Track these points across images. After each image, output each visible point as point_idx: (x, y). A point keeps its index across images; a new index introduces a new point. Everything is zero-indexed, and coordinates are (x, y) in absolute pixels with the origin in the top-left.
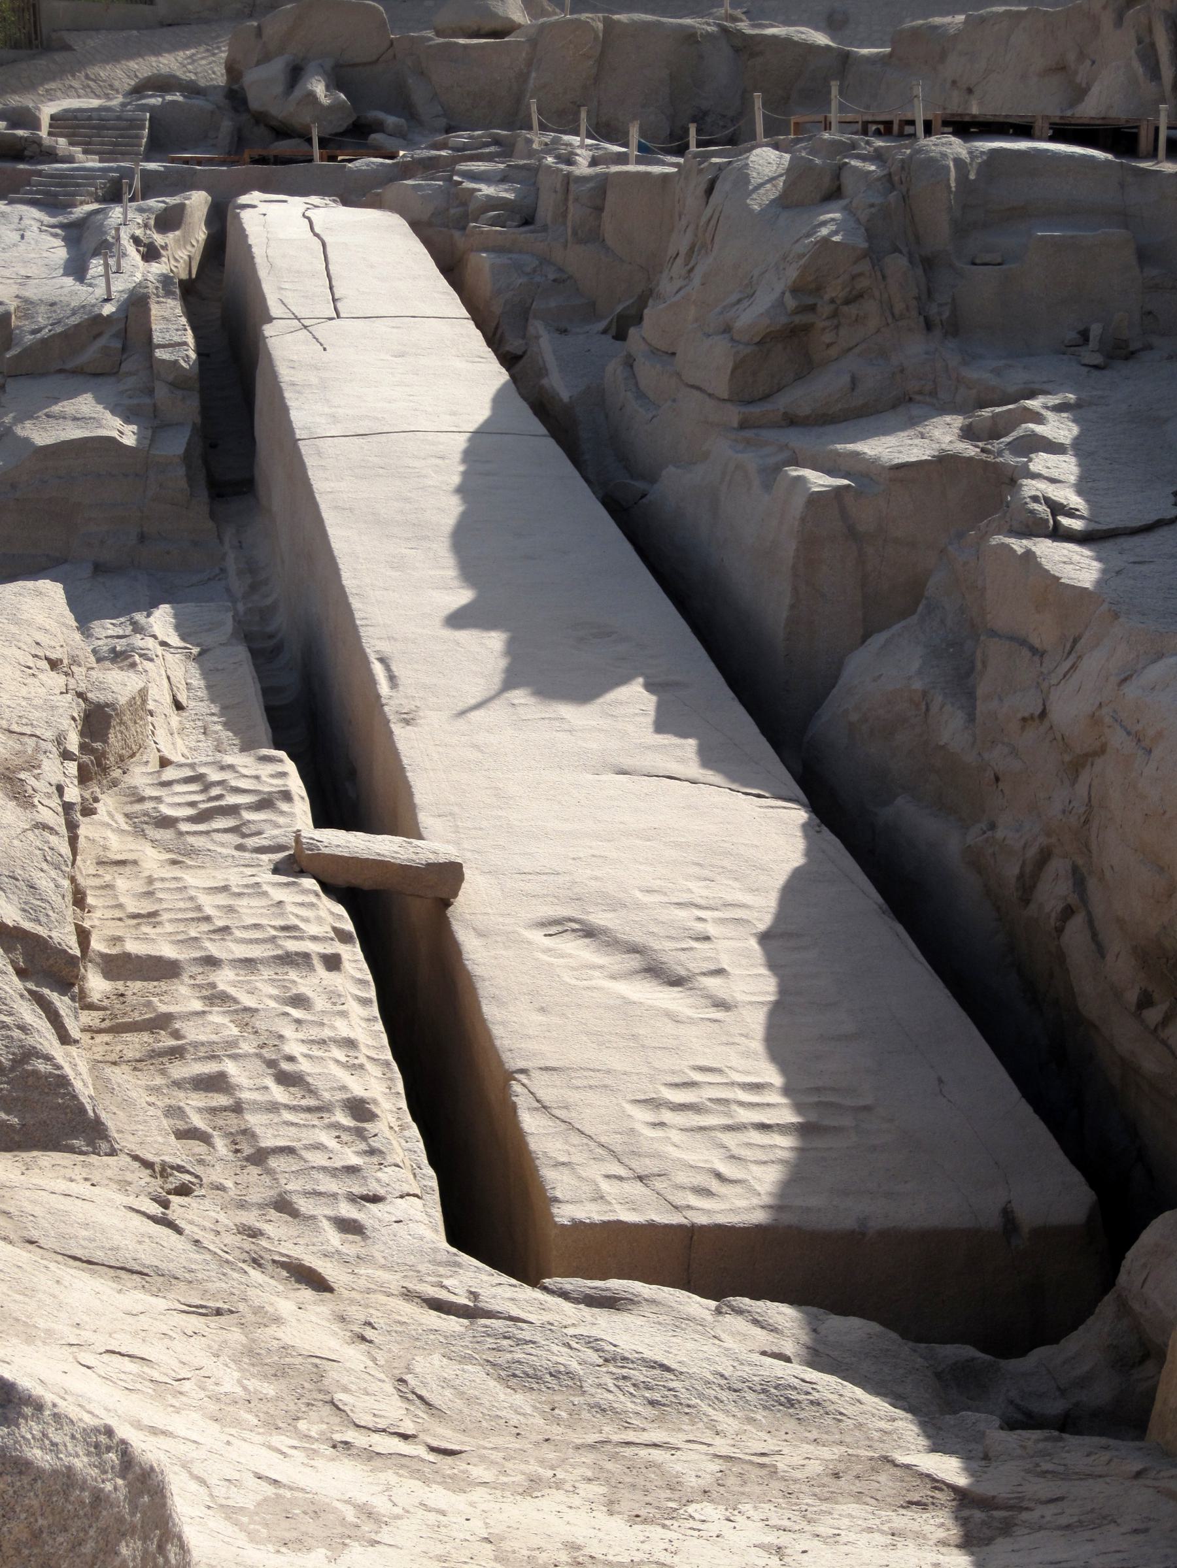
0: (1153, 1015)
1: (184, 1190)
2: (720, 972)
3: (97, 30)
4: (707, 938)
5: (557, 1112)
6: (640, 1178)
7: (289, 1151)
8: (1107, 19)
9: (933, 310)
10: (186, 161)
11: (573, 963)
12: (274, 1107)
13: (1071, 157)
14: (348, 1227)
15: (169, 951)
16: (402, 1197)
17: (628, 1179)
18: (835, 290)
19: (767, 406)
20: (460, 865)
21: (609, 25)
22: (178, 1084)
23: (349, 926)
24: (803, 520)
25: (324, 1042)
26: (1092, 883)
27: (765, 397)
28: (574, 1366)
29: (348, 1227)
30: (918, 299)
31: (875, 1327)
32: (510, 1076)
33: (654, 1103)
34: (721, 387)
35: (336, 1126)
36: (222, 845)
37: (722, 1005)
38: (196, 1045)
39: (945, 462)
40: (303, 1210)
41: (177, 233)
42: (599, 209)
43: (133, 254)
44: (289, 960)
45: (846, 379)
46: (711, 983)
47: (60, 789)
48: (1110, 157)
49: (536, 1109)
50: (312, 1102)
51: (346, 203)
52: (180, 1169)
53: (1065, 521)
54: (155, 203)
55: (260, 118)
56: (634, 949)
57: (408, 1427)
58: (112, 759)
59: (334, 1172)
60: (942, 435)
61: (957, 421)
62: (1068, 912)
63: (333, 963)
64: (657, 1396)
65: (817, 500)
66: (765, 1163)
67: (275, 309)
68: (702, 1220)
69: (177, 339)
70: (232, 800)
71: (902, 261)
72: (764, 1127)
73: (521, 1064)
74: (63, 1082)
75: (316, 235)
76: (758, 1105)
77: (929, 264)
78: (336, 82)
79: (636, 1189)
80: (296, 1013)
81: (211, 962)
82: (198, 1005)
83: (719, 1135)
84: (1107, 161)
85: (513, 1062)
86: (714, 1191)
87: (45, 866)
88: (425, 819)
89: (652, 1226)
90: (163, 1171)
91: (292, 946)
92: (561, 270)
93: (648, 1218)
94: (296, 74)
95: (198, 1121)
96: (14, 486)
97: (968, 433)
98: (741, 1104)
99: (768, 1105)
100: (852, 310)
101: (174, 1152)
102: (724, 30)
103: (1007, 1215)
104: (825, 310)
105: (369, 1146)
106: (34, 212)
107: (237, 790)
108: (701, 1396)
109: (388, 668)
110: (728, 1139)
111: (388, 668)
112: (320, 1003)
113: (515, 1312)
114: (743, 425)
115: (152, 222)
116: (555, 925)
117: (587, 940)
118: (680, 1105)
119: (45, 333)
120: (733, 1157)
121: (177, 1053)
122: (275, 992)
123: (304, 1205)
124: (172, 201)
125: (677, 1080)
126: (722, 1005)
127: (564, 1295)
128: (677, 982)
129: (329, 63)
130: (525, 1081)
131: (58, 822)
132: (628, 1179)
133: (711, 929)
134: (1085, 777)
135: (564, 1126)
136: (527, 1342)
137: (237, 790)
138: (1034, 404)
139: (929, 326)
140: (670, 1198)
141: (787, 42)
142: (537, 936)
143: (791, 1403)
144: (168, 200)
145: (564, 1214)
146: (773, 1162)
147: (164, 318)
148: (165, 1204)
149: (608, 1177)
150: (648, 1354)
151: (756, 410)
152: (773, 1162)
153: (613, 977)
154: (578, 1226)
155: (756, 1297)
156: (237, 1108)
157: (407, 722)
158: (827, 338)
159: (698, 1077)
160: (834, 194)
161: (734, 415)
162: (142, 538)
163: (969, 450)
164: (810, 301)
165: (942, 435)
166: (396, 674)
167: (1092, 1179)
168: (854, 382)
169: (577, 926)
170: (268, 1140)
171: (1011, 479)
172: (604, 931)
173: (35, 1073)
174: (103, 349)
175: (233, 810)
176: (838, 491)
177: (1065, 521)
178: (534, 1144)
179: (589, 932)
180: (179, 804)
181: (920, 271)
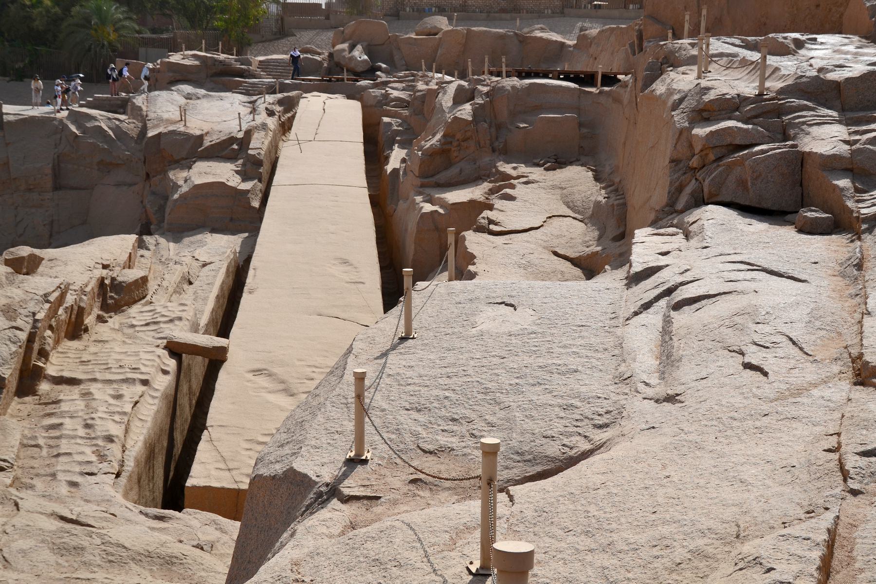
3: (306, 29)
4: (312, 379)
7: (69, 454)
9: (496, 144)
10: (303, 80)
11: (256, 386)
13: (561, 86)
14: (73, 484)
18: (459, 136)
19: (431, 179)
21: (469, 31)
24: (418, 223)
27: (432, 176)
30: (491, 140)
39: (472, 203)
42: (424, 102)
43: (264, 114)
45: (458, 170)
47: (34, 314)
48: (577, 86)
53: (492, 227)
56: (283, 382)
59: (80, 463)
64: (110, 558)
71: (486, 125)
77: (499, 127)
78: (368, 51)
79: (227, 473)
84: (575, 88)
85: (209, 423)
87: (8, 343)
89: (223, 489)
92: (409, 125)
94: (352, 47)
95: (41, 442)
96: (185, 199)
100: (464, 144)
102: (516, 34)
104: (455, 144)
107: (163, 316)
122: (112, 393)
125: (267, 432)
128: (292, 395)
129: (365, 44)
136: (73, 535)
137: (163, 316)
138: (512, 181)
139: (494, 151)
141: (541, 38)
142: (250, 376)
143: (173, 564)
151: (426, 180)
153: (270, 392)
157: (250, 293)
158: (455, 154)
161: (418, 182)
162: (231, 219)
164: (449, 140)
168: (461, 170)
172: (275, 374)
174: (230, 149)
176: (432, 212)
177: (492, 227)
178: (198, 455)
181: (493, 130)
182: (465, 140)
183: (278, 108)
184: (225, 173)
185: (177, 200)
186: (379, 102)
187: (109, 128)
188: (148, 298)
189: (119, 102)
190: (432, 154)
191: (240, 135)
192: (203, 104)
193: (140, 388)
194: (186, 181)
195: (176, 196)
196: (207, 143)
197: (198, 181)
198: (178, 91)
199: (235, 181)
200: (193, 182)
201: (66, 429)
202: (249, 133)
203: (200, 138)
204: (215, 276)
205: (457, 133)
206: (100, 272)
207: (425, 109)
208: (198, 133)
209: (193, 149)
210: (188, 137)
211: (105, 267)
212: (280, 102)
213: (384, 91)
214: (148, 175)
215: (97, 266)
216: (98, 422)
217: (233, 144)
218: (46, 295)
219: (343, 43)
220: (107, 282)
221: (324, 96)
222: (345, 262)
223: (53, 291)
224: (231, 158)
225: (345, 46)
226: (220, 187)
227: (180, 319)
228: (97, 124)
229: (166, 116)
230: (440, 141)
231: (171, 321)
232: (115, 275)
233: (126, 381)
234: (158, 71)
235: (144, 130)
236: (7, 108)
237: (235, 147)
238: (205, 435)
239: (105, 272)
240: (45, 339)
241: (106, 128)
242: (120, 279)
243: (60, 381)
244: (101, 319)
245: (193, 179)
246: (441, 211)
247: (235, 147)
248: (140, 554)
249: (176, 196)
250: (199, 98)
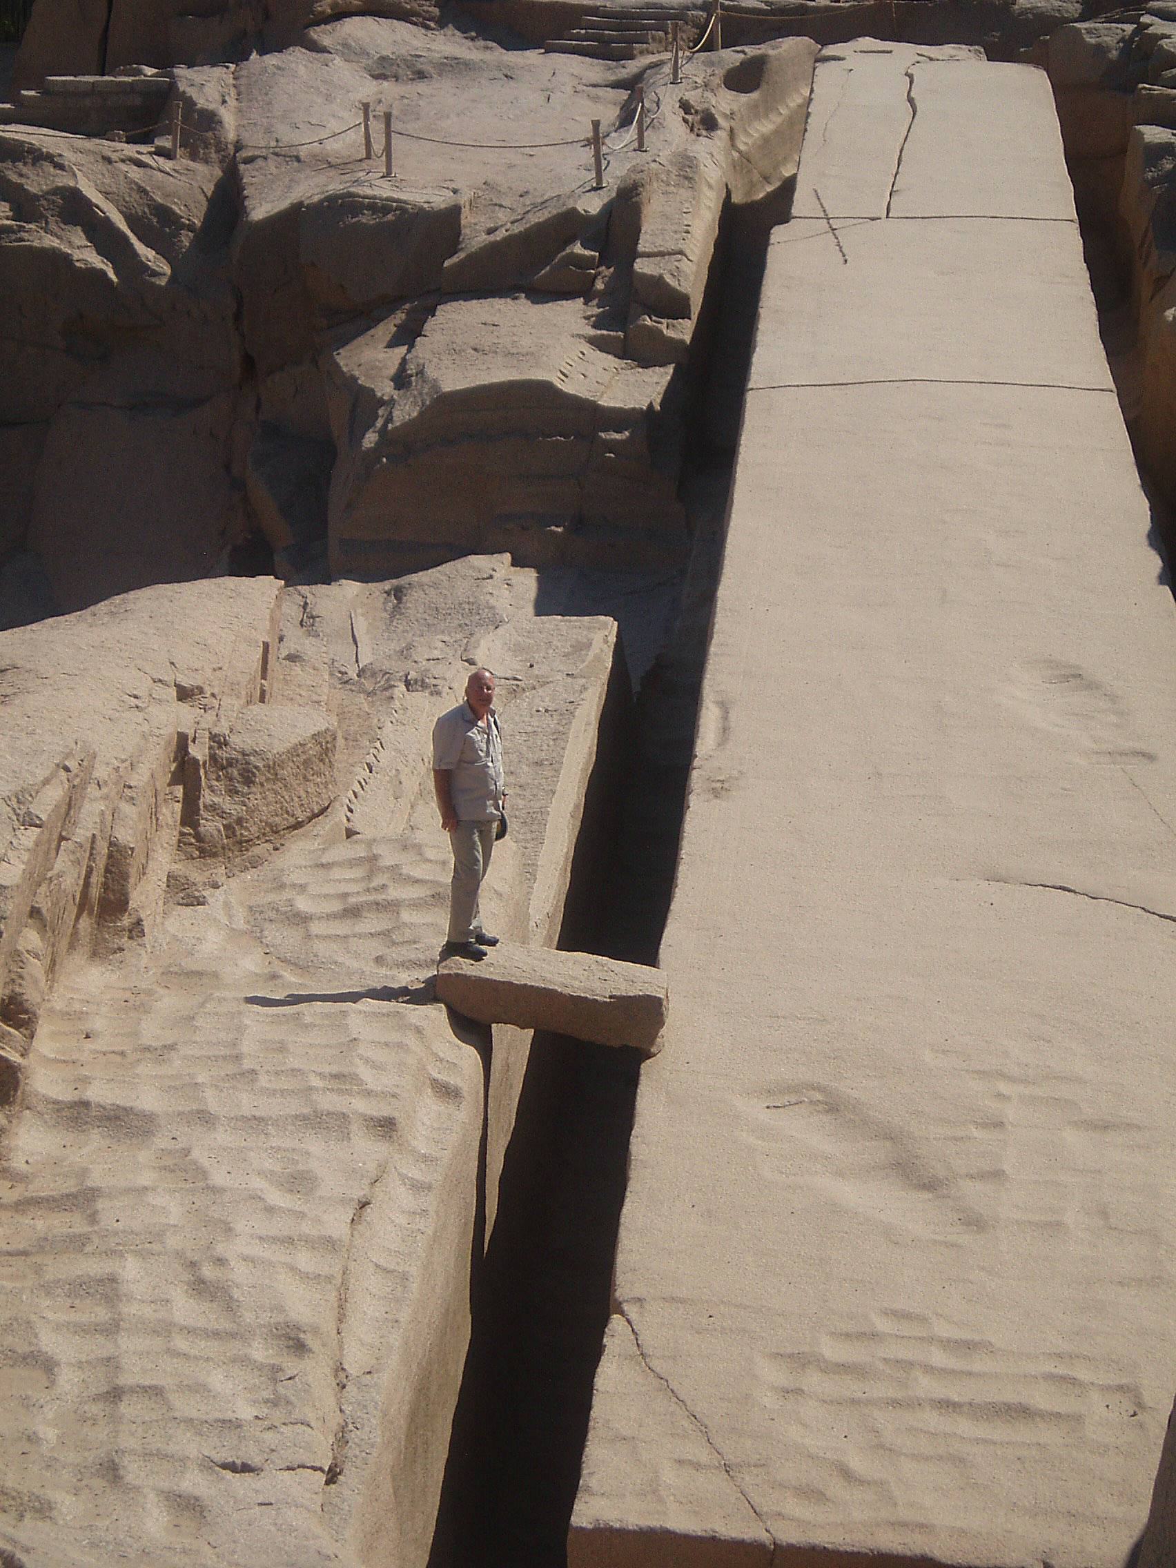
2: (997, 1175)
4: (999, 1125)
5: (655, 1363)
6: (727, 1468)
7: (155, 1392)
12: (165, 1329)
15: (148, 1100)
16: (289, 1469)
17: (707, 1467)
20: (658, 1002)
22: (48, 1289)
25: (290, 1240)
29: (188, 1507)
33: (801, 1361)
35: (244, 1361)
36: (357, 956)
37: (975, 1222)
40: (129, 1478)
41: (755, 95)
44: (317, 1121)
46: (973, 1192)
49: (631, 1357)
50: (225, 1324)
51: (995, 54)
54: (731, 57)
58: (254, 829)
66: (927, 1459)
68: (789, 1535)
69: (671, 246)
70: (394, 893)
73: (639, 1290)
75: (911, 100)
76: (953, 1372)
81: (205, 1118)
82: (146, 1178)
83: (876, 1413)
86: (828, 1494)
88: (675, 935)
91: (329, 1102)
93: (709, 1526)
98: (929, 1369)
99: (970, 1374)
105: (275, 1392)
109: (725, 718)
111: (725, 718)
112: (332, 1183)
115: (717, 80)
116: (788, 1096)
117: (826, 1118)
118: (838, 1365)
119: (500, 235)
120: (881, 1446)
121: (78, 1243)
124: (752, 51)
125: (850, 1327)
128: (931, 1185)
130: (633, 1316)
132: (707, 1467)
133: (1011, 1113)
135: (656, 1382)
140: (756, 1499)
142: (755, 1109)
144: (747, 49)
146: (940, 1458)
147: (664, 215)
149: (680, 1462)
152: (940, 1458)
153: (840, 1174)
156: (112, 1329)
157: (716, 794)
159: (883, 1325)
166: (732, 724)
169: (819, 1096)
175: (392, 907)
178: (600, 1409)
179: (832, 1106)
180: (326, 896)
187: (106, 194)
188: (339, 814)
189: (138, 101)
191: (593, 205)
192: (440, 95)
193: (367, 1149)
197: (453, 380)
198: (350, 52)
200: (435, 386)
201: (130, 1298)
204: (559, 737)
208: (439, 200)
209: (419, 262)
213: (1129, 28)
214: (249, 363)
215: (159, 692)
216: (240, 1273)
217: (570, 240)
220: (198, 752)
221: (905, 52)
223: (46, 782)
228: (64, 180)
229: (304, 140)
232: (222, 728)
235: (228, 198)
238: (616, 1334)
239: (185, 717)
240: (22, 963)
241: (95, 197)
243: (76, 1114)
244: (184, 894)
245: (431, 372)
249: (370, 439)
250: (421, 75)
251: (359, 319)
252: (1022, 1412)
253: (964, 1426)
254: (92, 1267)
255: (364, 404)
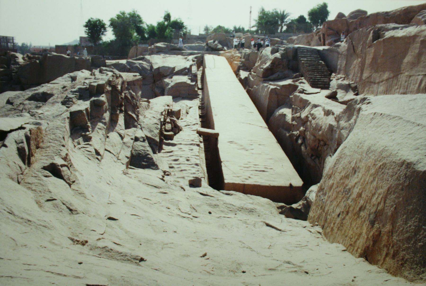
0: (313, 158)
1: (168, 175)
8: (315, 35)
12: (184, 164)
23: (202, 140)
26: (305, 140)
27: (267, 77)
28: (219, 204)
31: (269, 200)
32: (222, 162)
34: (261, 76)
38: (176, 155)
39: (290, 85)
45: (277, 75)
52: (168, 172)
53: (305, 92)
55: (210, 47)
56: (242, 146)
57: (190, 213)
59: (191, 174)
60: (289, 82)
61: (292, 80)
62: (302, 144)
63: (198, 145)
65: (272, 89)
67: (207, 66)
68: (246, 183)
70: (189, 124)
72: (256, 171)
74: (152, 159)
79: (237, 178)
80: (191, 151)
85: (222, 160)
90: (165, 172)
94: (214, 42)
97: (293, 81)
101: (167, 169)
103: (291, 185)
106: (180, 56)
108: (238, 210)
110: (252, 172)
113: (212, 195)
114: (264, 80)
123: (186, 178)
126: (252, 154)
127: (223, 193)
131: (160, 124)
134: (305, 125)
143: (253, 212)
145: (226, 181)
148: (163, 177)
150: (231, 203)
151: (265, 79)
154: (228, 183)
155: (251, 194)
157: (216, 115)
160: (277, 51)
161: (263, 79)
162: (189, 94)
163: (293, 83)
165: (289, 82)
167: (303, 180)
168: (278, 76)
170: (183, 169)
171: (297, 87)
173: (148, 157)
176: (276, 88)
177: (305, 92)
182: (279, 65)
183: (196, 60)
184: (185, 79)
185: (170, 88)
186: (230, 57)
190: (267, 70)
194: (172, 82)
195: (170, 86)
196: (176, 70)
199: (189, 82)
202: (191, 66)
203: (174, 68)
205: (275, 62)
206: (167, 108)
207: (250, 58)
209: (171, 72)
210: (169, 68)
211: (168, 106)
212: (196, 58)
218: (162, 113)
219: (211, 40)
220: (170, 111)
222: (244, 106)
224: (185, 74)
225: (212, 41)
226: (185, 83)
227: (197, 124)
230: (269, 65)
231: (194, 125)
233: (191, 144)
234: (153, 49)
235: (152, 67)
236: (107, 61)
237: (187, 71)
241: (139, 66)
242: (173, 110)
246: (279, 88)
247: (187, 71)
248: (240, 208)
251: (166, 77)
252: (264, 171)
253: (257, 172)
254: (177, 158)
255: (168, 84)
